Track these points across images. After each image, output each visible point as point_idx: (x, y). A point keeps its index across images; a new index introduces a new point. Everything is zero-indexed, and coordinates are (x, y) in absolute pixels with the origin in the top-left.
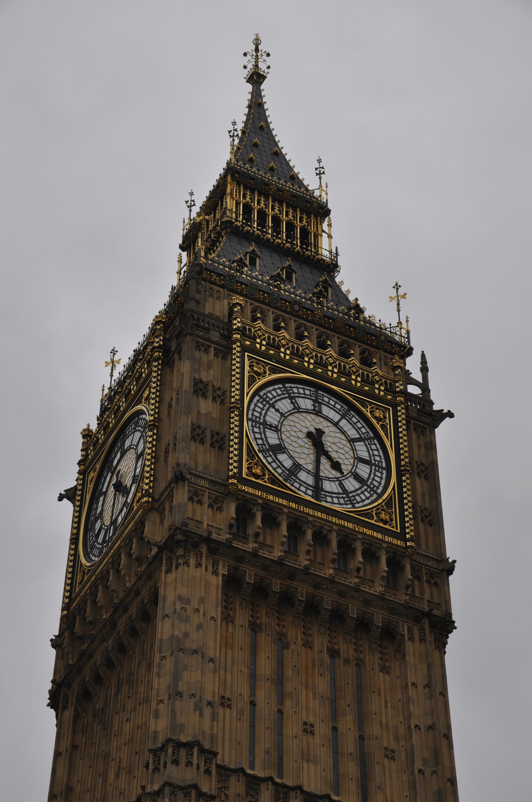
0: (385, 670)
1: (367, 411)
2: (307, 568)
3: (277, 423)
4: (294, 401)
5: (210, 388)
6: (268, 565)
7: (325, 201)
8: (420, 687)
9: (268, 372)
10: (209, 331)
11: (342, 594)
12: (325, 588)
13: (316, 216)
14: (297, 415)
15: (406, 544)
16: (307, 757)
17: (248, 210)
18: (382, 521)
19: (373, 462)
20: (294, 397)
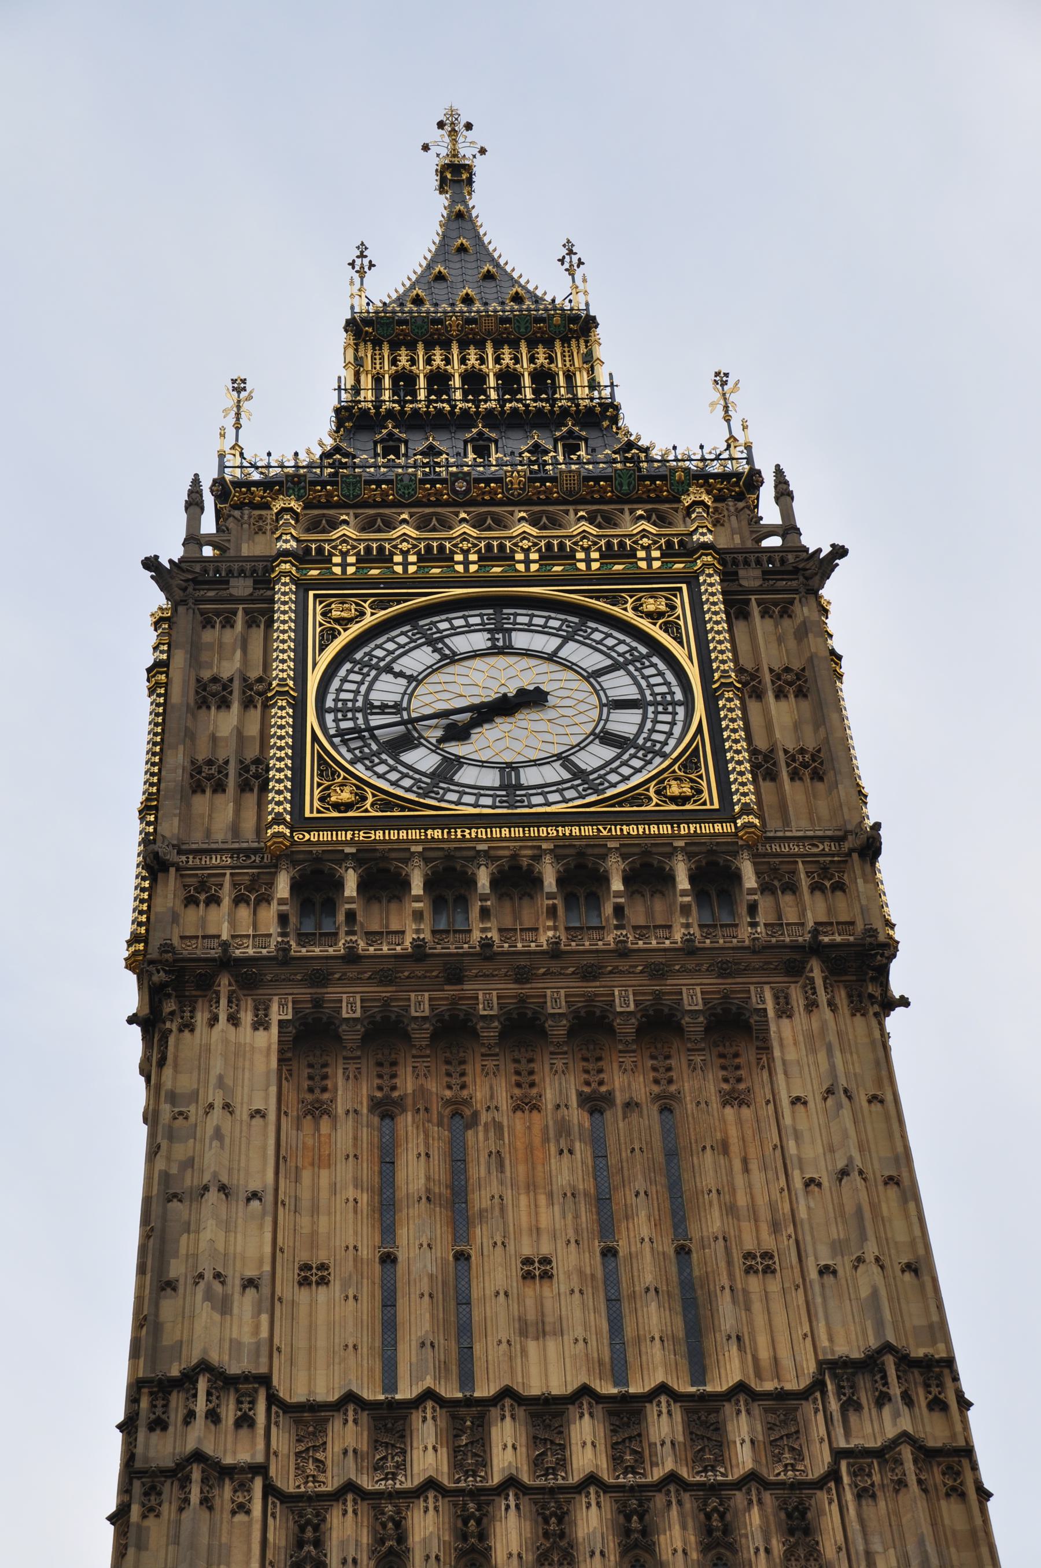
0: (735, 1098)
1: (625, 609)
2: (486, 944)
3: (398, 698)
4: (440, 645)
5: (236, 685)
6: (387, 971)
7: (583, 306)
8: (815, 1102)
9: (369, 611)
10: (227, 582)
11: (589, 974)
12: (544, 974)
13: (566, 341)
14: (450, 669)
15: (736, 824)
16: (534, 1328)
17: (404, 382)
18: (674, 799)
19: (649, 698)
20: (441, 640)
